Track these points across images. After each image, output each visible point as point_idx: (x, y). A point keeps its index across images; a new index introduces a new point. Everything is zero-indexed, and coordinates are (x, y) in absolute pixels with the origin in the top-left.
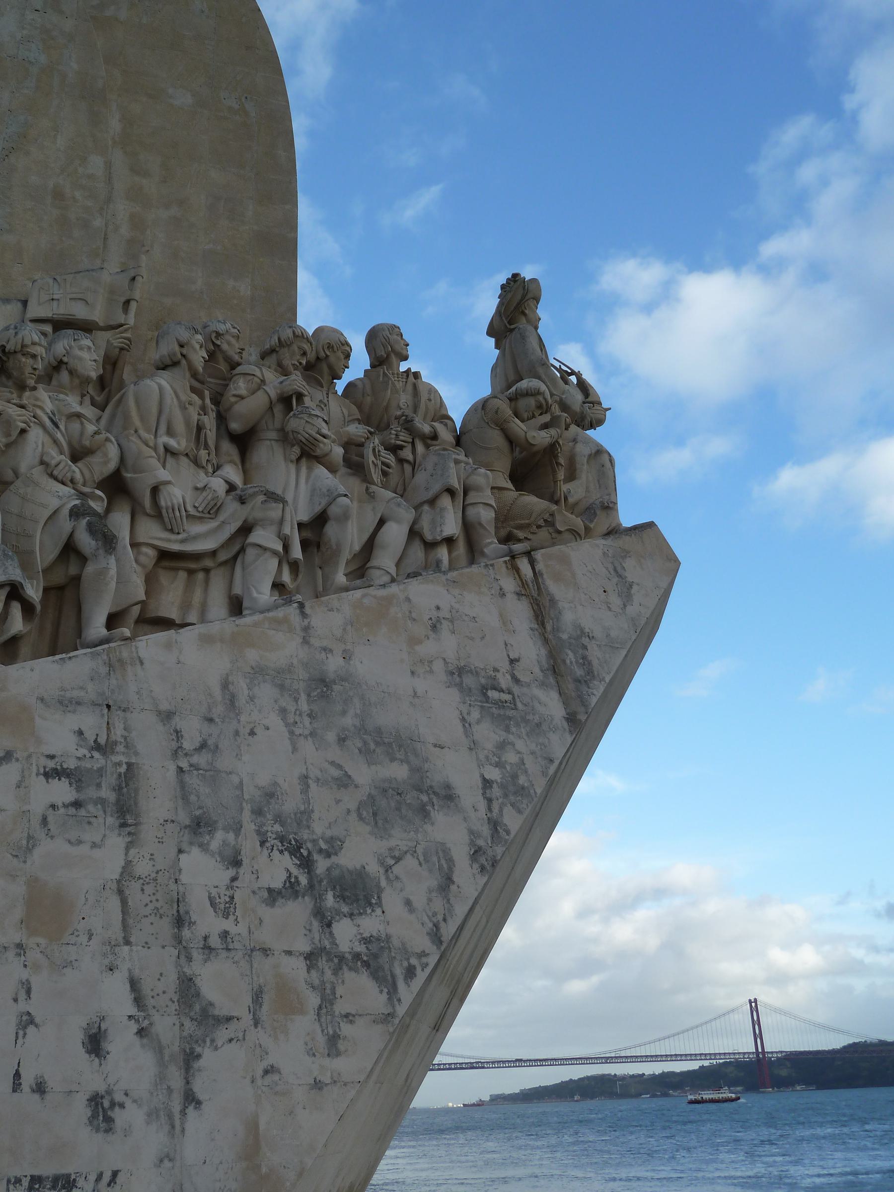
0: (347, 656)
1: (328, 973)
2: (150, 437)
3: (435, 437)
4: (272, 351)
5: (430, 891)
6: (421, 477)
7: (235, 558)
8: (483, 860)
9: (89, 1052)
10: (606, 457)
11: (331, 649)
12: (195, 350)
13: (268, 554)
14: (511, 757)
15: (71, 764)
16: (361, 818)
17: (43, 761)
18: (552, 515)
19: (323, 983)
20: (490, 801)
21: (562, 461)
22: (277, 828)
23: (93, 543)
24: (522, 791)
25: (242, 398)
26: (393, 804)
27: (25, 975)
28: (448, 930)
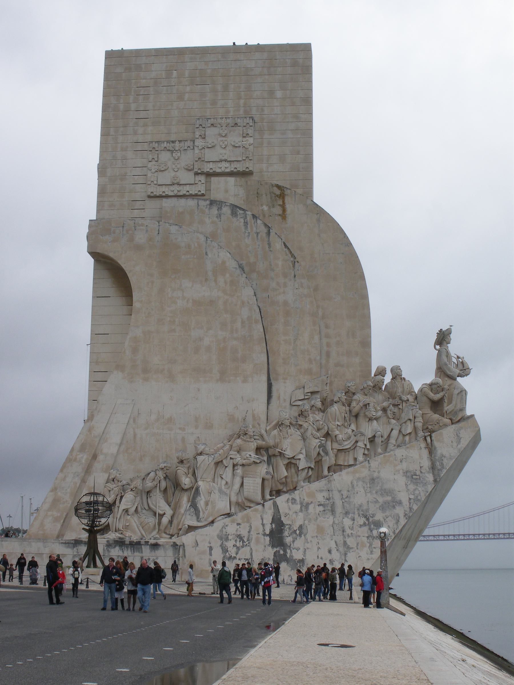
0: (379, 472)
1: (371, 540)
3: (408, 400)
5: (394, 524)
6: (403, 415)
7: (355, 448)
8: (407, 516)
9: (329, 553)
10: (464, 392)
11: (375, 471)
12: (343, 398)
13: (361, 448)
14: (417, 492)
15: (323, 503)
16: (380, 509)
17: (318, 503)
19: (370, 542)
20: (410, 503)
21: (446, 401)
22: (362, 512)
24: (419, 500)
25: (355, 407)
26: (387, 506)
27: (318, 541)
28: (397, 531)
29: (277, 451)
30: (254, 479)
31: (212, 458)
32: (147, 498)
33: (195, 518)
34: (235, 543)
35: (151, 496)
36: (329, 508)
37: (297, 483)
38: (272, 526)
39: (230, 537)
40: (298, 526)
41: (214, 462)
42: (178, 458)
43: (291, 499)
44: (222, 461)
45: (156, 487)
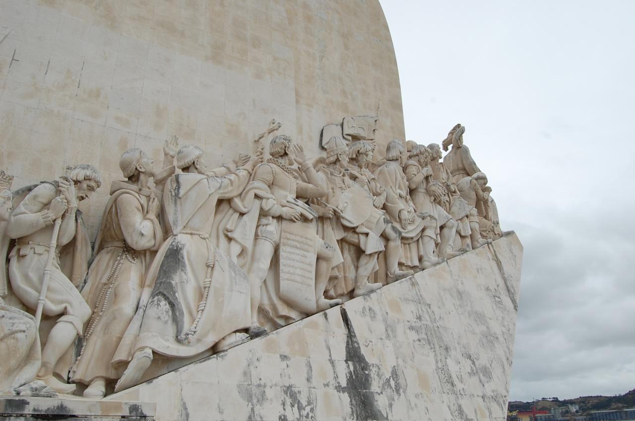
1: (488, 403)
2: (394, 189)
4: (417, 155)
7: (418, 240)
13: (432, 240)
18: (493, 227)
20: (505, 339)
23: (395, 234)
25: (415, 175)
29: (331, 209)
30: (302, 252)
31: (218, 182)
32: (8, 260)
33: (171, 330)
34: (283, 412)
35: (24, 256)
36: (424, 336)
37: (356, 280)
38: (348, 367)
39: (269, 393)
40: (390, 370)
41: (219, 195)
42: (124, 167)
43: (367, 308)
44: (229, 201)
45: (50, 227)
